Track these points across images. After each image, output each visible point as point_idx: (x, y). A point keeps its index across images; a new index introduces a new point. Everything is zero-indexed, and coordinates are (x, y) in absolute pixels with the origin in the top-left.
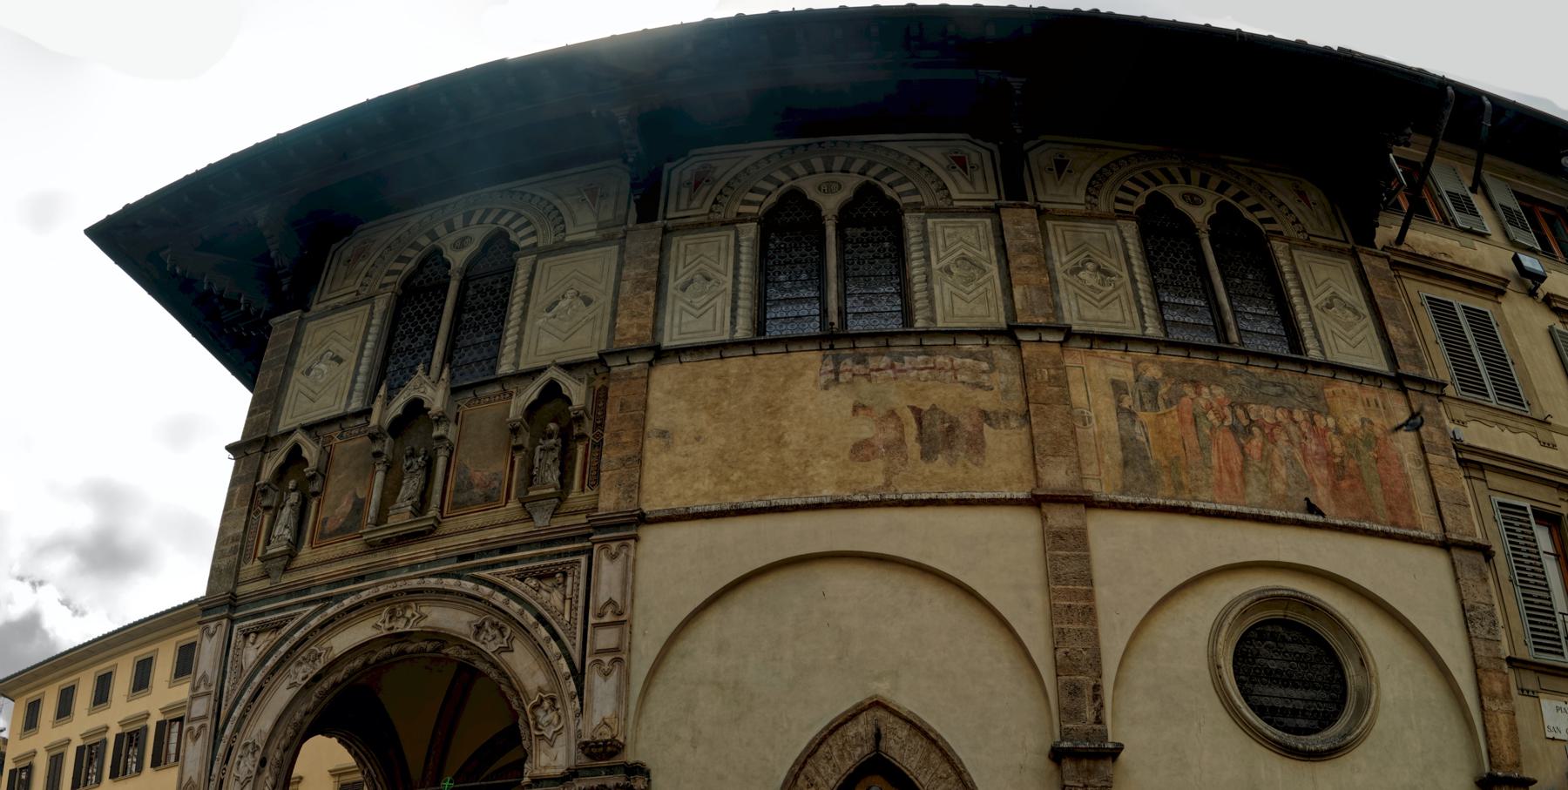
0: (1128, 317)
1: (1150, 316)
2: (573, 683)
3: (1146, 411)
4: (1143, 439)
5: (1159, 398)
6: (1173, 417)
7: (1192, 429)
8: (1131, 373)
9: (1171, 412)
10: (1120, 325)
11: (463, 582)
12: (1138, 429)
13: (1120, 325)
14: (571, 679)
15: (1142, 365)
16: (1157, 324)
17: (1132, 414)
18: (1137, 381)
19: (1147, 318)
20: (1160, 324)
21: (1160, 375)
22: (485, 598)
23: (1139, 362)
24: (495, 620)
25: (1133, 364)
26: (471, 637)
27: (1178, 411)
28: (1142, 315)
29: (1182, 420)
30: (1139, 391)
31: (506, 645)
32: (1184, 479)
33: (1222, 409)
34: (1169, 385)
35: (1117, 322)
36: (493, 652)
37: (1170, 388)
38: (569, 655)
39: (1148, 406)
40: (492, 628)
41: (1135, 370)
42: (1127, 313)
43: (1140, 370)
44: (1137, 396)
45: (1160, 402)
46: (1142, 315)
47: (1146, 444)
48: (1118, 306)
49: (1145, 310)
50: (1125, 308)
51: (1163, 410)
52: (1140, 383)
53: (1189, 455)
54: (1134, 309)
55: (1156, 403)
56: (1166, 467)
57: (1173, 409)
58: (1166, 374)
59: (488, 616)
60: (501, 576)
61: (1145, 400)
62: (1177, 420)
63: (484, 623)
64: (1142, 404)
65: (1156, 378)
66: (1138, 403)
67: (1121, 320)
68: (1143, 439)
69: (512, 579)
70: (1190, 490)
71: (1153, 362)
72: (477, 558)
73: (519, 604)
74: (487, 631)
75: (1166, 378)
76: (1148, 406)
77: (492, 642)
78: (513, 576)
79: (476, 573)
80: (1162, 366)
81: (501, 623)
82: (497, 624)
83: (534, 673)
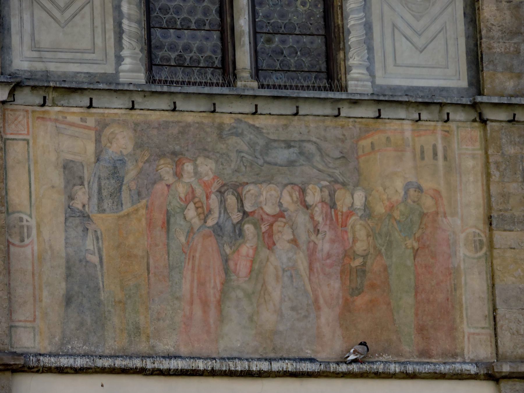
0: (99, 42)
1: (130, 37)
3: (104, 211)
4: (94, 259)
5: (124, 187)
6: (140, 220)
7: (159, 234)
8: (91, 147)
9: (137, 210)
10: (87, 56)
12: (90, 244)
13: (87, 56)
15: (108, 131)
16: (137, 50)
17: (85, 217)
18: (98, 160)
19: (126, 41)
20: (141, 50)
21: (130, 147)
23: (106, 125)
25: (96, 131)
27: (147, 207)
28: (119, 32)
29: (150, 224)
30: (99, 178)
32: (142, 320)
33: (208, 198)
34: (141, 164)
35: (83, 52)
37: (141, 169)
39: (107, 204)
41: (98, 141)
42: (99, 31)
43: (104, 140)
44: (95, 187)
45: (125, 195)
46: (119, 32)
47: (99, 267)
48: (87, 20)
49: (125, 23)
50: (98, 22)
51: (127, 208)
52: (102, 163)
53: (152, 280)
54: (110, 25)
55: (120, 197)
56: (120, 302)
57: (139, 205)
58: (139, 146)
61: (105, 193)
62: (144, 222)
64: (101, 200)
65: (125, 152)
66: (95, 200)
67: (89, 46)
68: (94, 259)
70: (148, 337)
71: (124, 124)
75: (138, 151)
76: (107, 204)
80: (135, 130)
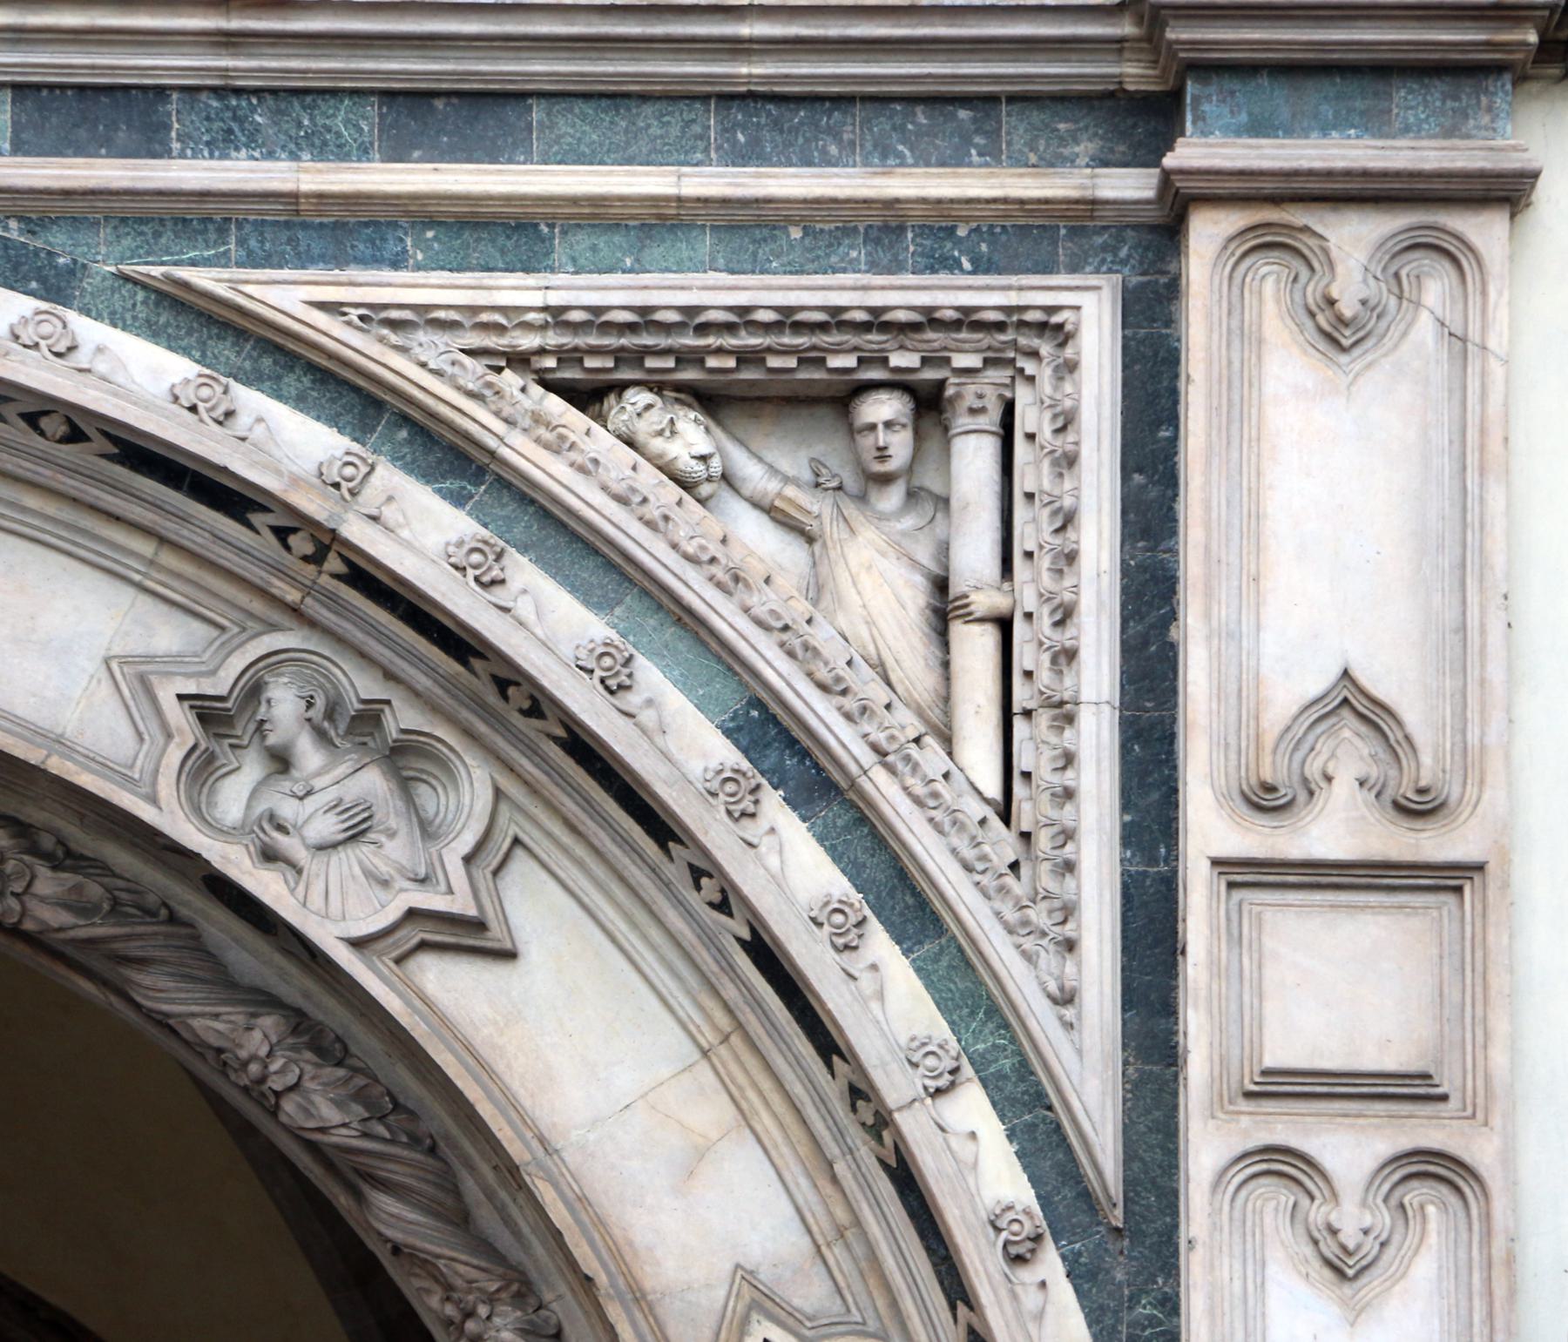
2: (1064, 1293)
11: (89, 331)
14: (1051, 1264)
22: (313, 505)
24: (363, 685)
26: (166, 786)
31: (461, 904)
36: (358, 944)
38: (1024, 1069)
40: (321, 736)
59: (289, 639)
60: (429, 343)
63: (253, 692)
69: (510, 380)
72: (192, 147)
73: (596, 602)
74: (281, 761)
77: (347, 861)
78: (519, 360)
79: (204, 278)
81: (404, 717)
82: (369, 718)
83: (701, 1153)
